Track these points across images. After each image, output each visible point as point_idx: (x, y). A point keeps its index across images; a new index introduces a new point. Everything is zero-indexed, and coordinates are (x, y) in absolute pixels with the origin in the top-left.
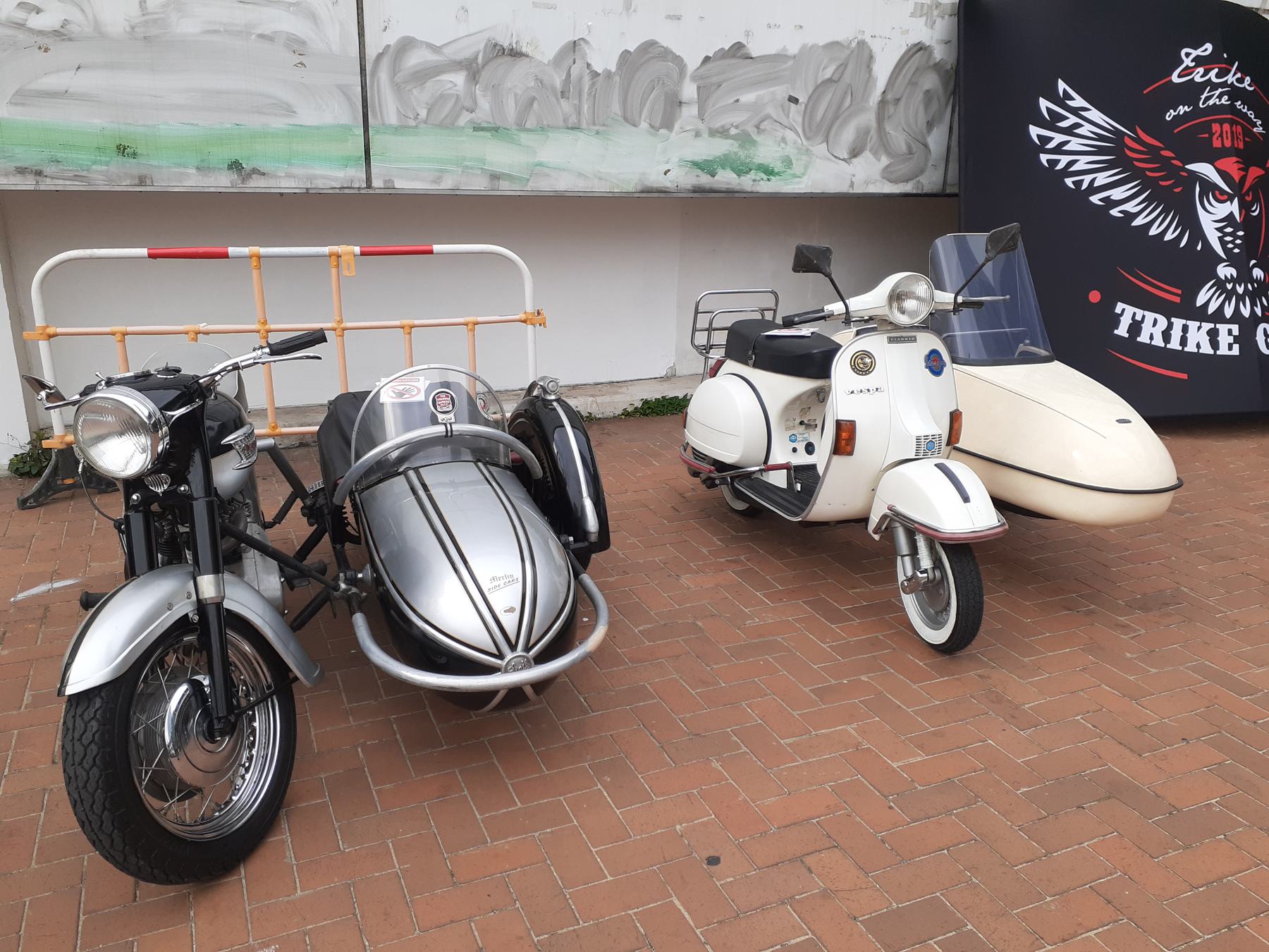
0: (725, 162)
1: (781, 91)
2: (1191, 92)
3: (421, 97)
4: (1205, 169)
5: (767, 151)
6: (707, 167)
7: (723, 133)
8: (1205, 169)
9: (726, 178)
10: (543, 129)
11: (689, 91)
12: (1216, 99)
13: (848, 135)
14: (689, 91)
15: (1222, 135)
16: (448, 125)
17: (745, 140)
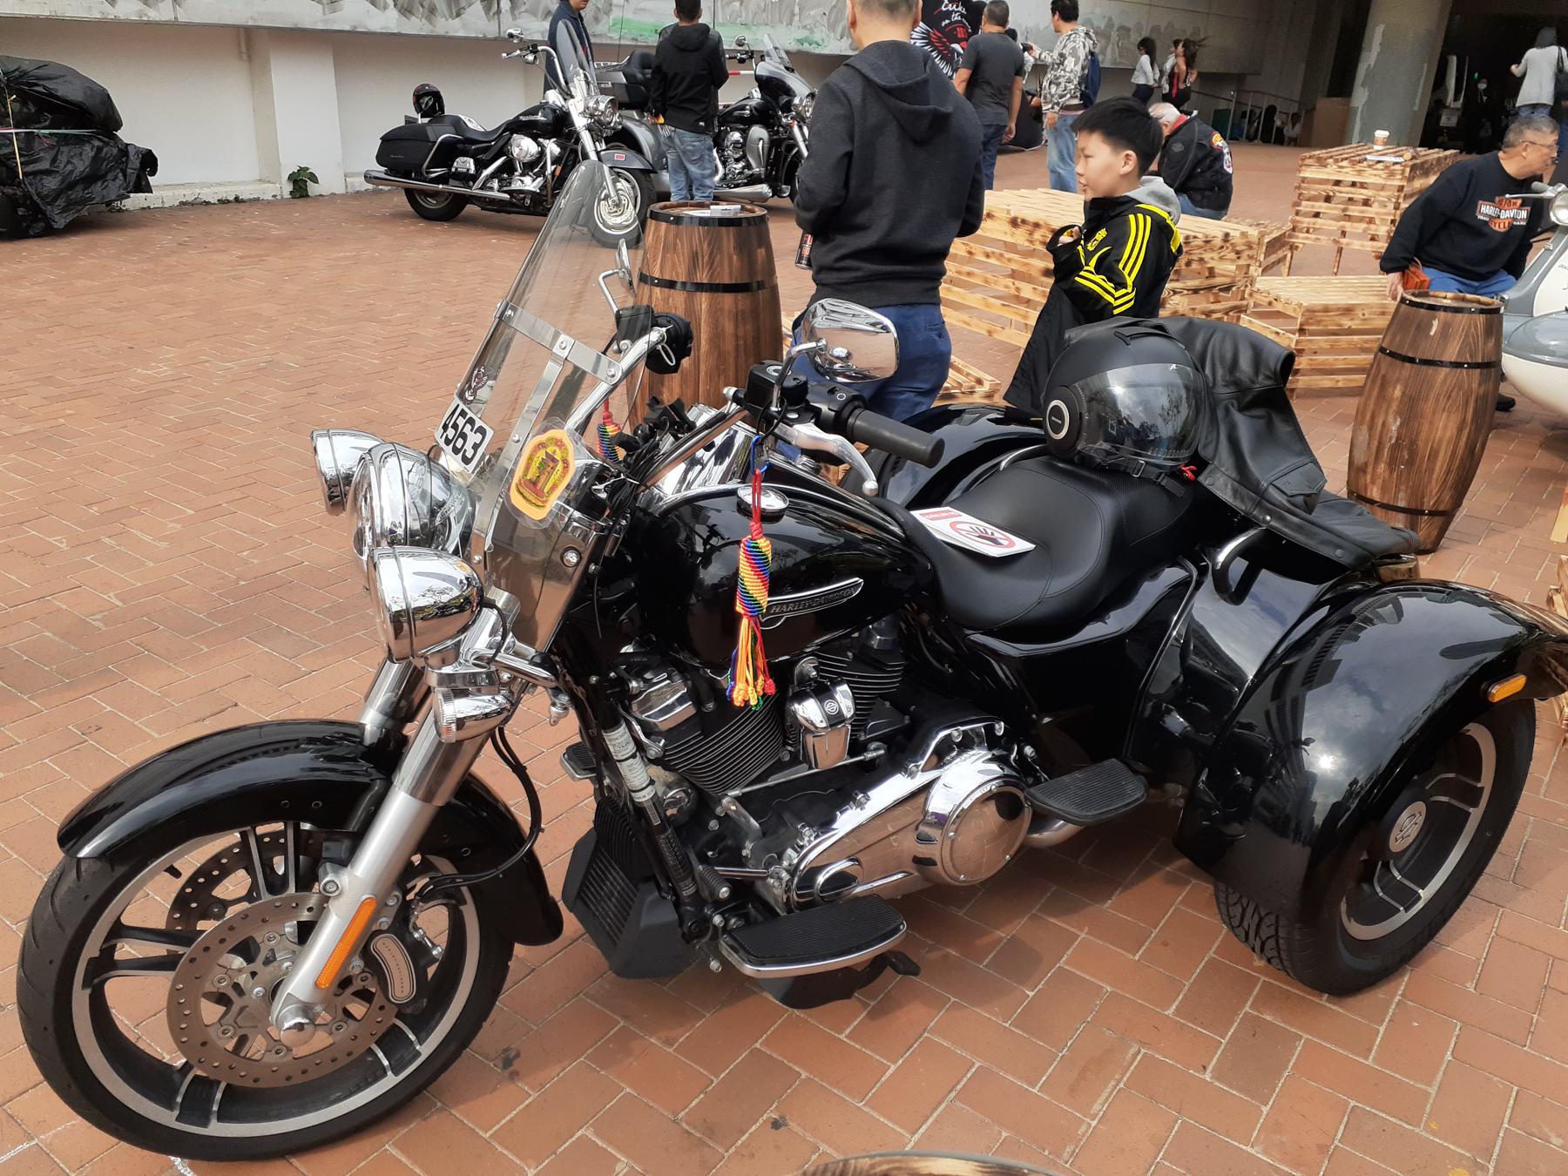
0: (806, 40)
1: (821, 10)
2: (948, 14)
3: (728, 11)
4: (955, 46)
5: (817, 37)
6: (800, 41)
7: (805, 27)
8: (955, 46)
9: (806, 47)
10: (757, 25)
11: (797, 10)
12: (955, 17)
13: (839, 30)
14: (797, 10)
15: (960, 33)
16: (734, 23)
17: (812, 32)
